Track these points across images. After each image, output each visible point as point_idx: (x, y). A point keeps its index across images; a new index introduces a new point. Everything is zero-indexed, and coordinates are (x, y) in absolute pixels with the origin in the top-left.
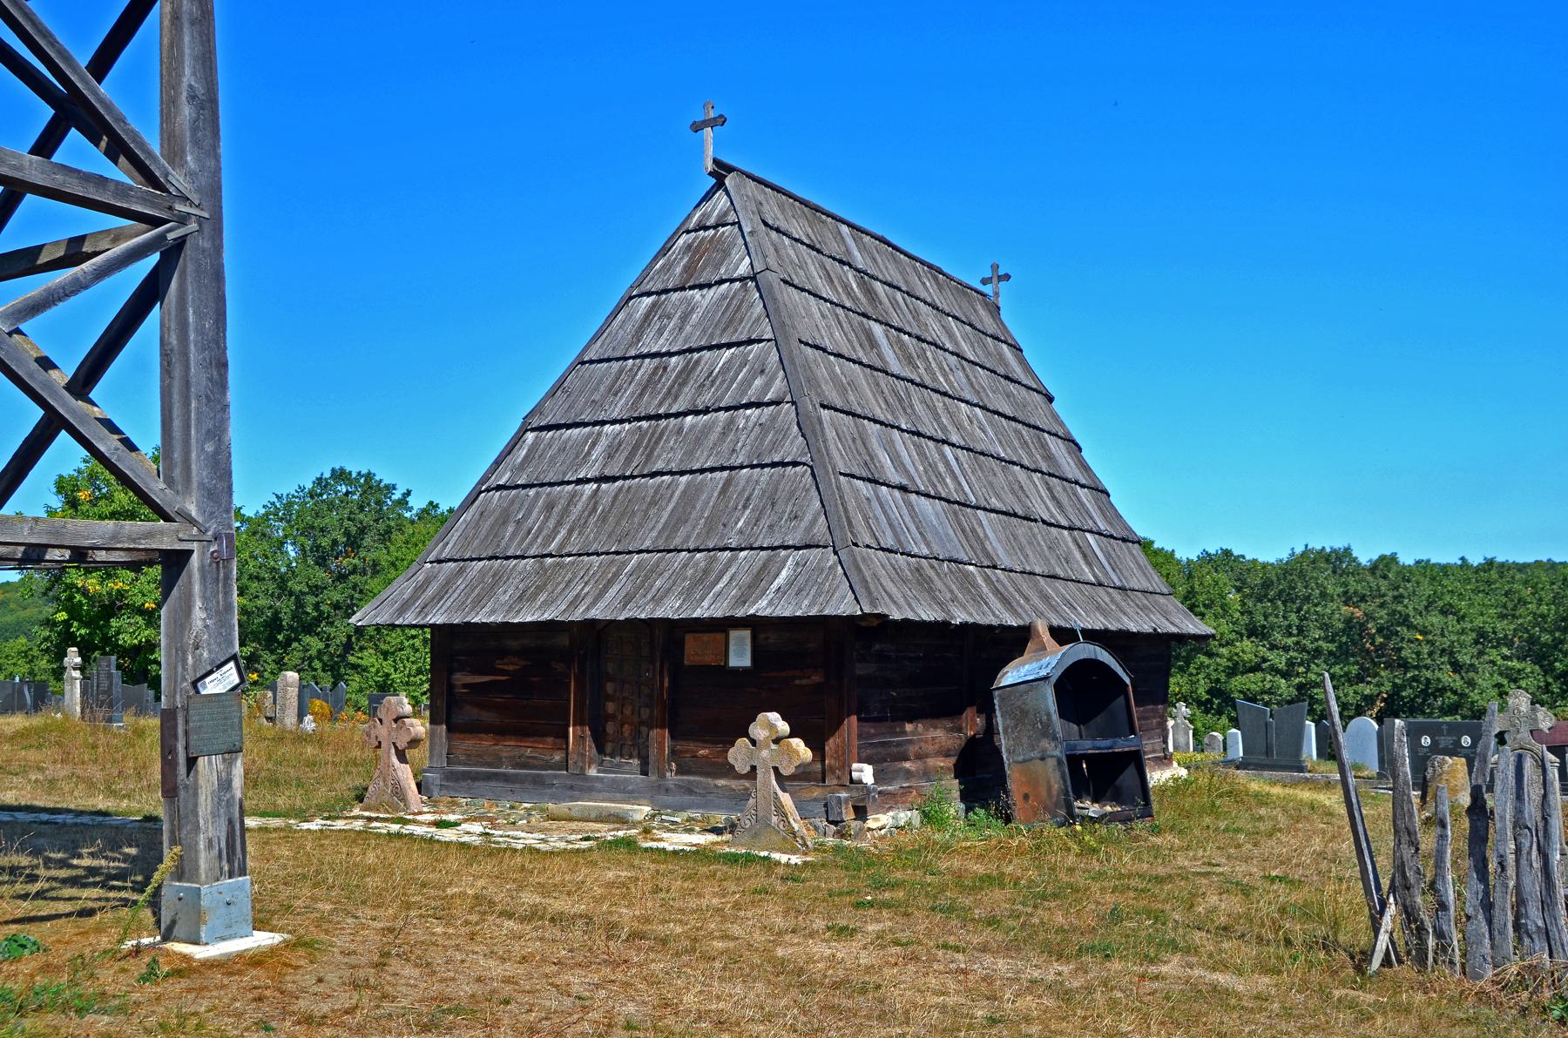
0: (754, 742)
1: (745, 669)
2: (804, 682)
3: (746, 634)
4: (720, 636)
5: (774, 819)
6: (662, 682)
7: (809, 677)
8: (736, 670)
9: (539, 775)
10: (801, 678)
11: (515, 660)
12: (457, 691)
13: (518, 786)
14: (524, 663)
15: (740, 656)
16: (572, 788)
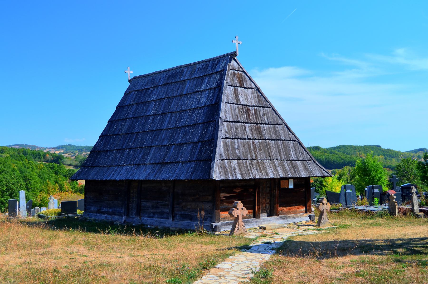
1: (292, 189)
3: (292, 180)
4: (287, 181)
7: (303, 190)
10: (301, 190)
12: (222, 199)
15: (291, 186)
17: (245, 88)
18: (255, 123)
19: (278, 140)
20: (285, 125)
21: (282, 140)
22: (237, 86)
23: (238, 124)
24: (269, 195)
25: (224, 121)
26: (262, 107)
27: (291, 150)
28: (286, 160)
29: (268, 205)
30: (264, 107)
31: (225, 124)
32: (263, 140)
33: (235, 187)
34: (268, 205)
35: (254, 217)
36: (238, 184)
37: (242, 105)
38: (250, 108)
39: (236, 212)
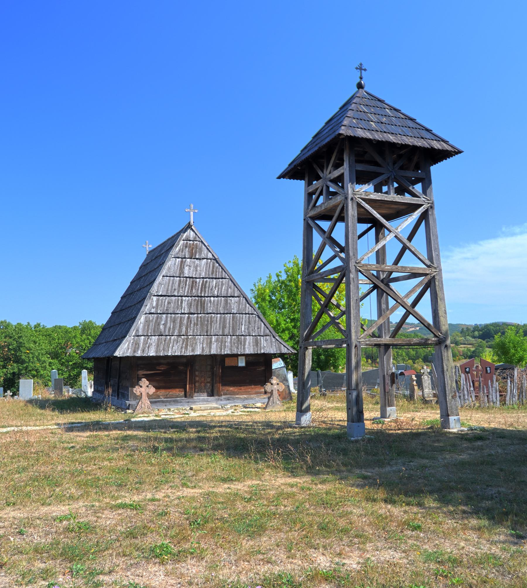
0: (272, 384)
1: (243, 367)
2: (260, 369)
3: (244, 358)
4: (236, 358)
5: (278, 402)
6: (219, 370)
8: (240, 367)
9: (176, 400)
11: (164, 366)
13: (168, 404)
14: (167, 367)
15: (242, 363)
16: (188, 402)
17: (197, 259)
18: (198, 296)
19: (227, 314)
20: (244, 297)
21: (233, 314)
22: (185, 258)
23: (173, 298)
24: (210, 373)
25: (154, 296)
26: (216, 278)
27: (242, 325)
28: (231, 336)
29: (209, 385)
30: (219, 278)
31: (155, 298)
32: (204, 314)
33: (159, 364)
34: (209, 385)
35: (186, 396)
36: (162, 361)
37: (186, 277)
38: (198, 280)
39: (138, 390)
